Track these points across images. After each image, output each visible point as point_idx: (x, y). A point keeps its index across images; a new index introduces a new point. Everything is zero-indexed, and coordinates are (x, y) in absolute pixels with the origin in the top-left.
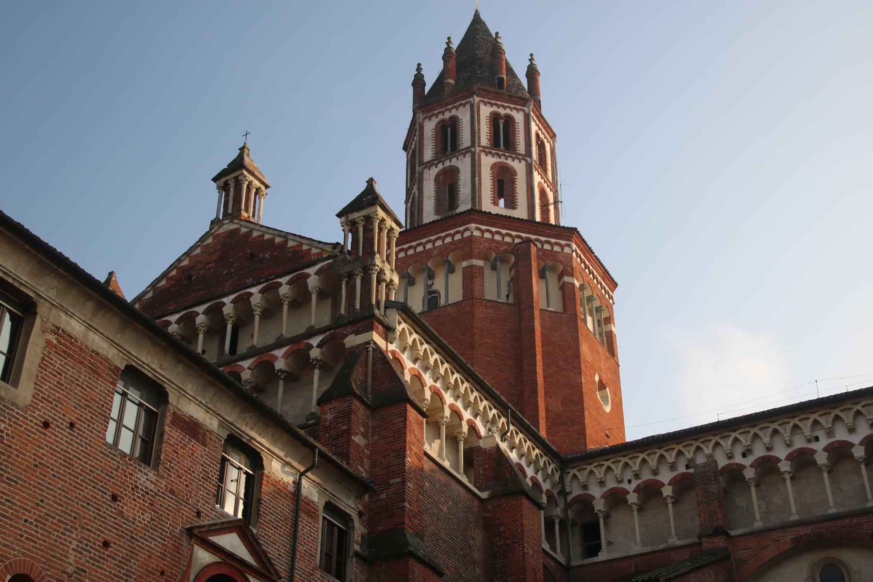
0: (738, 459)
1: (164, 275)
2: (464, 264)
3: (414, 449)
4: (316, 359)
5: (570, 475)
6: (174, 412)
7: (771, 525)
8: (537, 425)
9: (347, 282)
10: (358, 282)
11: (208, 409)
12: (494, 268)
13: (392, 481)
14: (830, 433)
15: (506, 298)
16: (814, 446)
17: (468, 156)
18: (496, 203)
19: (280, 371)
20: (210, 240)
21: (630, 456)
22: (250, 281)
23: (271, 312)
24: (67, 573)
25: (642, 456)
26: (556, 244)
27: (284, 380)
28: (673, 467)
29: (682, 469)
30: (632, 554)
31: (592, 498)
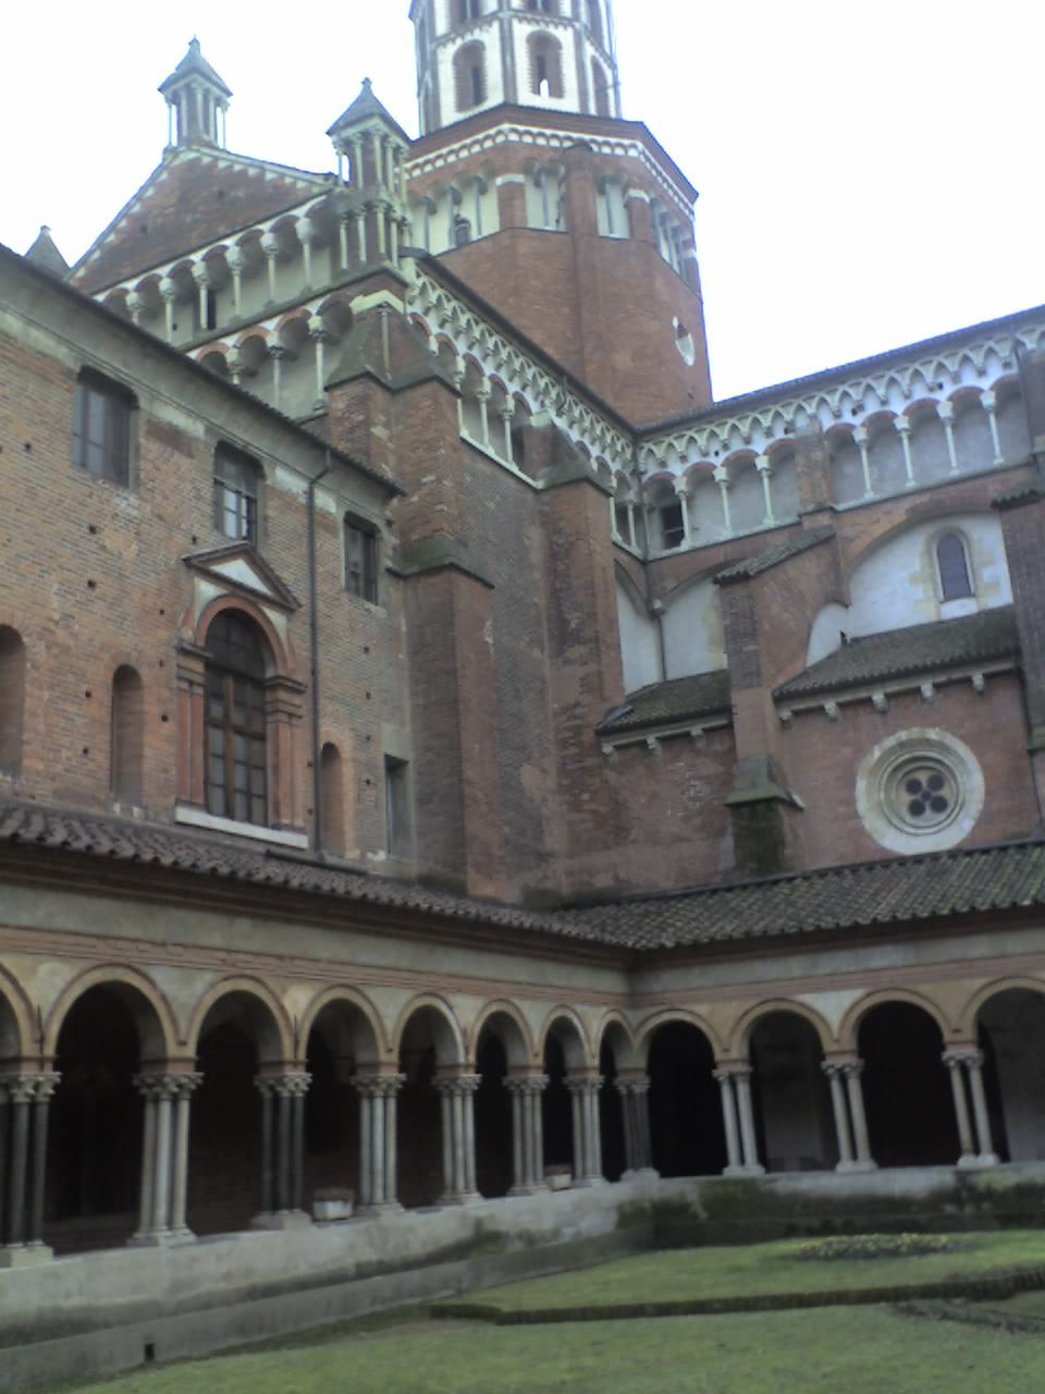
0: (848, 418)
1: (112, 228)
3: (448, 438)
4: (316, 331)
5: (645, 450)
6: (149, 421)
7: (885, 495)
9: (347, 224)
10: (361, 224)
11: (189, 413)
12: (538, 184)
13: (425, 480)
14: (956, 378)
15: (554, 224)
17: (496, 25)
18: (537, 91)
19: (273, 348)
20: (164, 176)
22: (222, 230)
23: (254, 269)
24: (51, 620)
25: (731, 421)
27: (280, 358)
28: (769, 433)
29: (780, 435)
30: (722, 539)
31: (673, 476)
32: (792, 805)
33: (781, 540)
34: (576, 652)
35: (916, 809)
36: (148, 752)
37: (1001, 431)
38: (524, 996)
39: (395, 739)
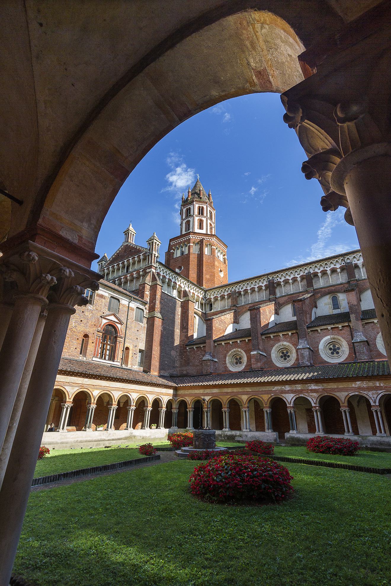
0: (240, 290)
1: (114, 255)
2: (189, 245)
10: (150, 257)
14: (258, 284)
16: (255, 287)
23: (134, 264)
26: (211, 239)
28: (227, 291)
29: (229, 292)
35: (237, 363)
36: (88, 348)
38: (148, 394)
39: (142, 346)
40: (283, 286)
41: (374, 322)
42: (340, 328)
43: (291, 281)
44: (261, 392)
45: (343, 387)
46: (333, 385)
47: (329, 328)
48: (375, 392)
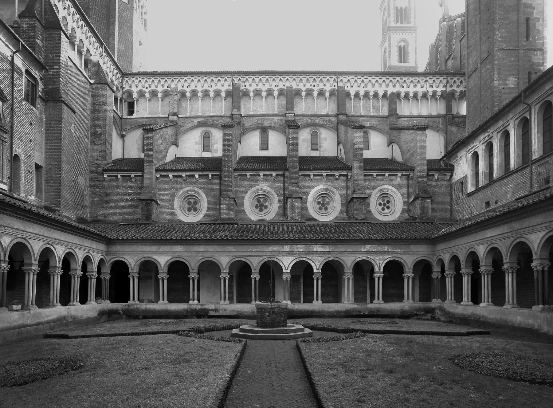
0: (185, 88)
7: (192, 116)
8: (114, 55)
16: (210, 89)
21: (148, 78)
28: (163, 86)
29: (166, 88)
32: (157, 202)
33: (162, 121)
34: (99, 142)
37: (225, 105)
40: (252, 98)
41: (372, 175)
42: (337, 177)
43: (264, 94)
44: (250, 253)
45: (351, 251)
46: (341, 248)
47: (325, 174)
48: (381, 257)
